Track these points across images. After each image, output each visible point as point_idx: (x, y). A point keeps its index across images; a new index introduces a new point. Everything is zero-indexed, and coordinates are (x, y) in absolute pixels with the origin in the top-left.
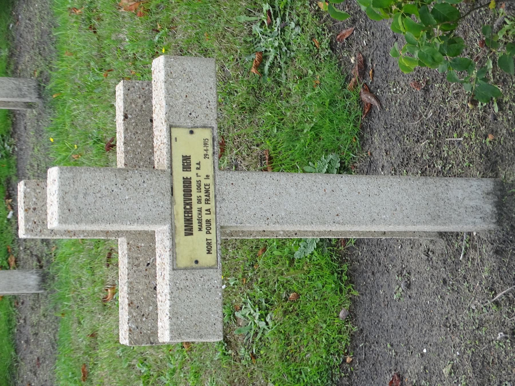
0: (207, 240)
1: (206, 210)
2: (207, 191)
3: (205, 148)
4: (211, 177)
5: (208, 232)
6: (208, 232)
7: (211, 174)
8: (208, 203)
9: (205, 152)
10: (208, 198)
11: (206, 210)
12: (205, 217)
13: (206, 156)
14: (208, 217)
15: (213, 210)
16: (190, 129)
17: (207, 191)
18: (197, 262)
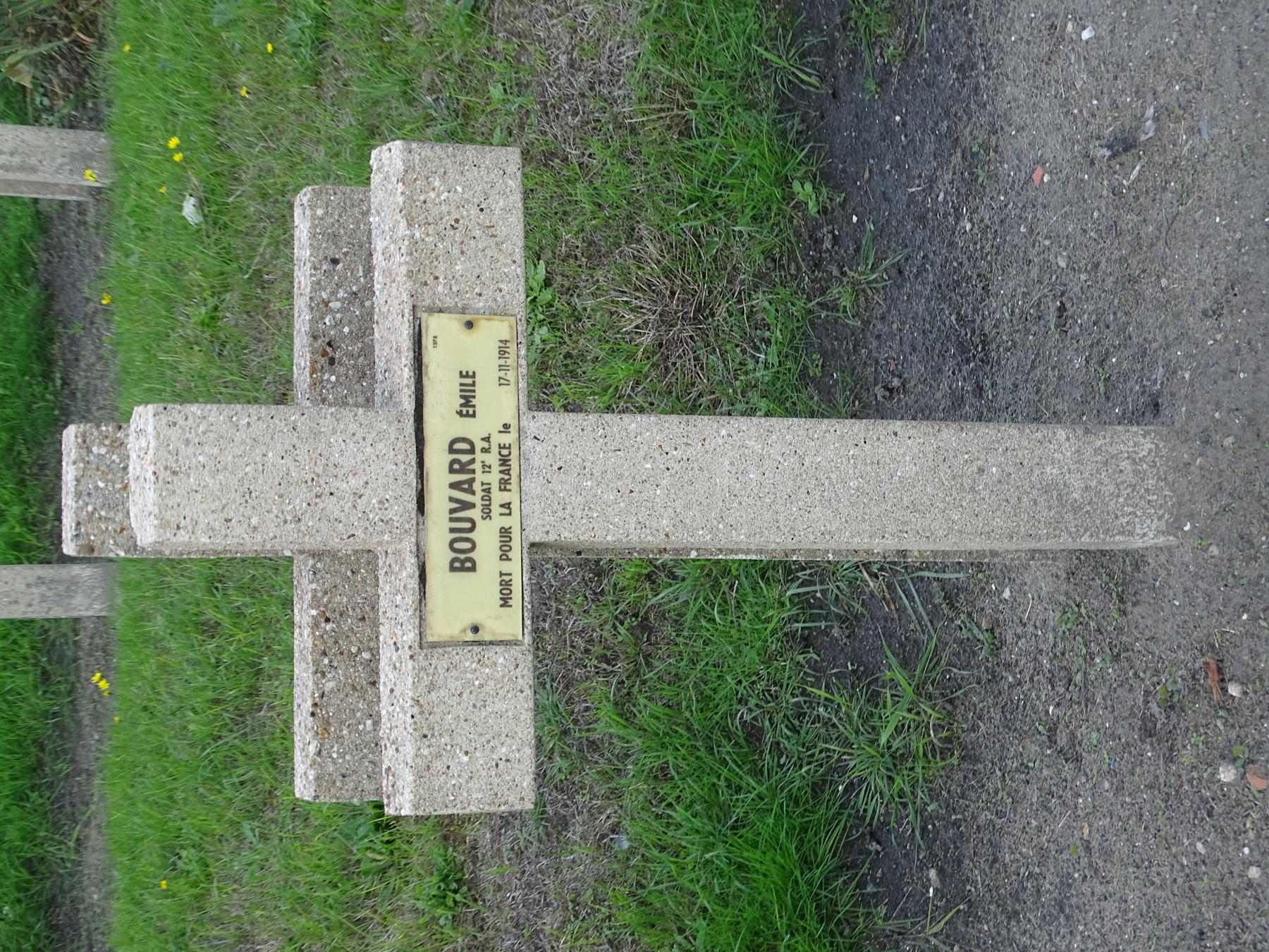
0: (501, 574)
1: (502, 506)
2: (504, 461)
3: (502, 362)
4: (513, 429)
5: (504, 557)
6: (504, 557)
8: (505, 490)
9: (502, 374)
10: (506, 477)
11: (502, 506)
12: (498, 521)
13: (503, 382)
14: (506, 522)
15: (515, 507)
16: (468, 317)
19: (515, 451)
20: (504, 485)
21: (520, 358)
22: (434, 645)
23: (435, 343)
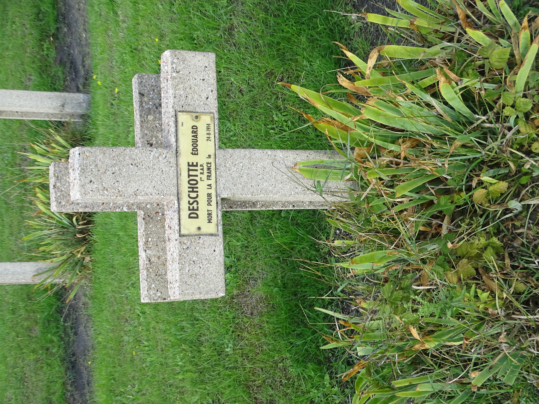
0: (208, 211)
1: (208, 185)
2: (209, 169)
3: (208, 132)
4: (213, 156)
5: (209, 204)
6: (209, 204)
7: (212, 153)
9: (208, 136)
11: (208, 185)
13: (208, 139)
14: (210, 191)
15: (213, 186)
16: (195, 114)
17: (209, 169)
18: (199, 228)
19: (212, 164)
20: (209, 177)
21: (214, 130)
22: (184, 236)
23: (182, 124)
